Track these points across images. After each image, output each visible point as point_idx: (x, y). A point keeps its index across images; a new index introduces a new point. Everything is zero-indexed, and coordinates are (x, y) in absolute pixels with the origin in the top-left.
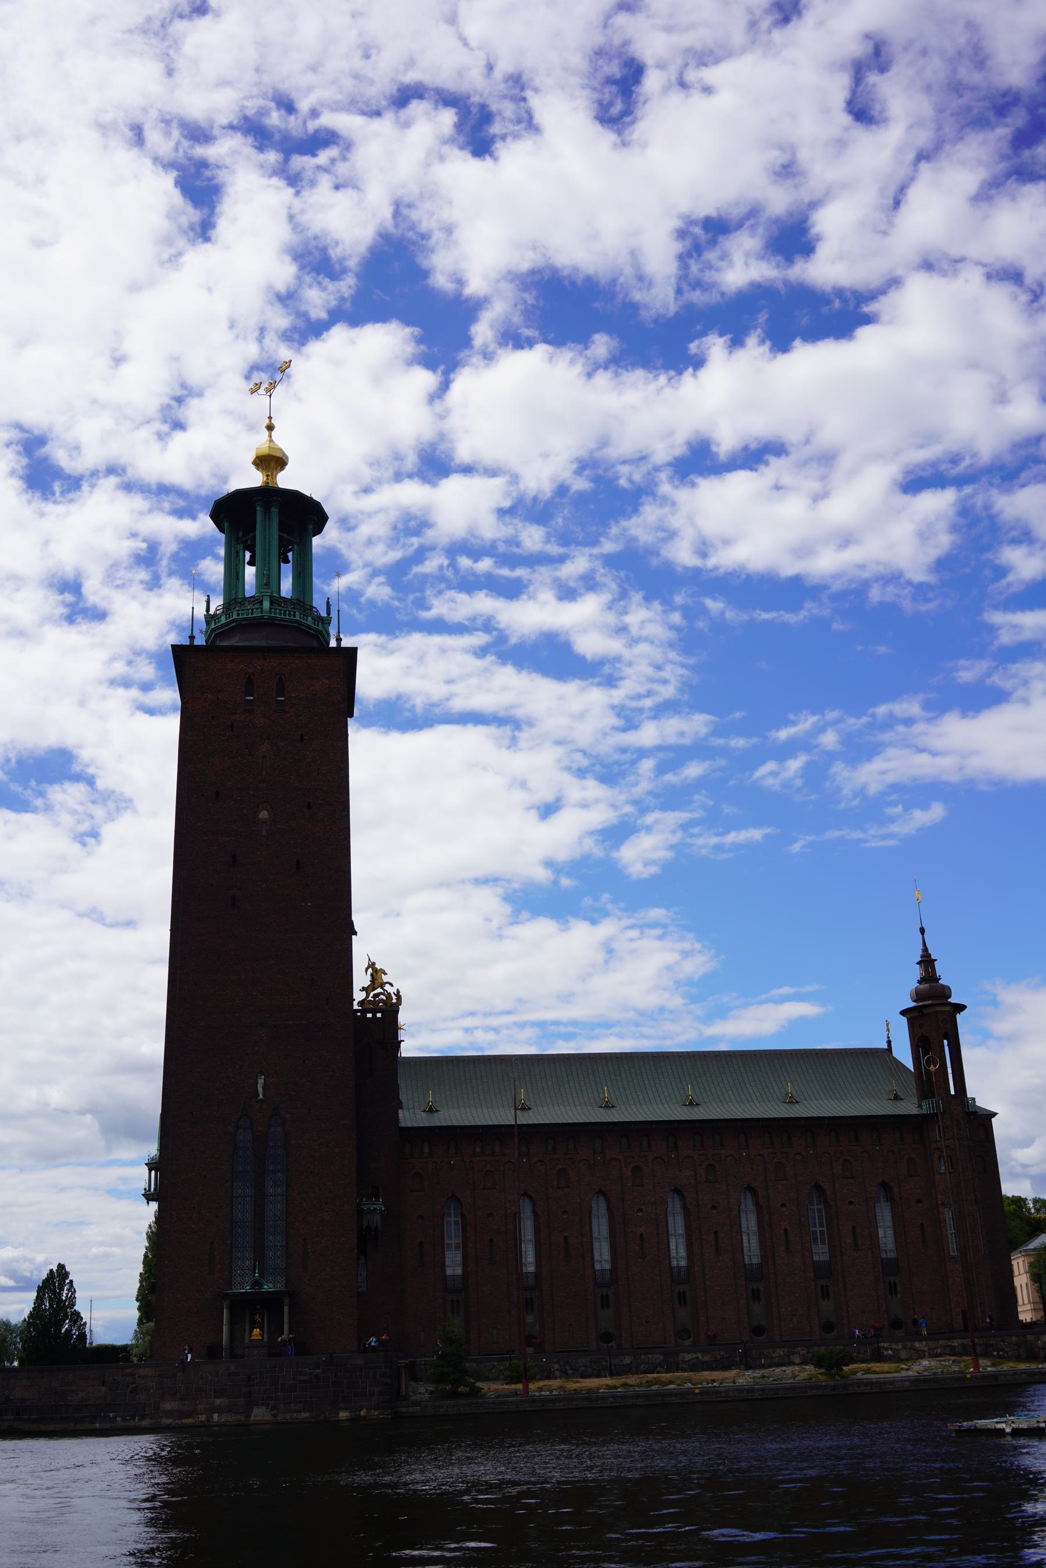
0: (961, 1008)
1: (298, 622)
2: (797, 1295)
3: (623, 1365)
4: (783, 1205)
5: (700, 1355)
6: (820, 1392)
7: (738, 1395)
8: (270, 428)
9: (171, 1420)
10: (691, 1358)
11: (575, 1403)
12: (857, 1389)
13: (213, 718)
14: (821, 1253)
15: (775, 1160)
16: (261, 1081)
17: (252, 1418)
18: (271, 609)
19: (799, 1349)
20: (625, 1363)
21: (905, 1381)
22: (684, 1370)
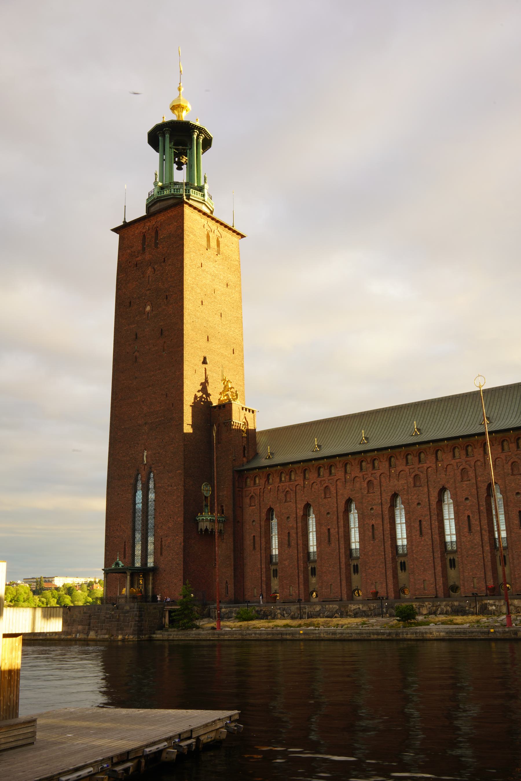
1: (173, 194)
3: (315, 612)
4: (467, 499)
5: (361, 606)
6: (380, 637)
7: (326, 636)
8: (180, 90)
9: (64, 636)
10: (355, 608)
11: (235, 636)
13: (129, 262)
15: (461, 467)
16: (145, 454)
17: (89, 637)
18: (158, 192)
19: (427, 603)
21: (441, 632)
22: (350, 616)
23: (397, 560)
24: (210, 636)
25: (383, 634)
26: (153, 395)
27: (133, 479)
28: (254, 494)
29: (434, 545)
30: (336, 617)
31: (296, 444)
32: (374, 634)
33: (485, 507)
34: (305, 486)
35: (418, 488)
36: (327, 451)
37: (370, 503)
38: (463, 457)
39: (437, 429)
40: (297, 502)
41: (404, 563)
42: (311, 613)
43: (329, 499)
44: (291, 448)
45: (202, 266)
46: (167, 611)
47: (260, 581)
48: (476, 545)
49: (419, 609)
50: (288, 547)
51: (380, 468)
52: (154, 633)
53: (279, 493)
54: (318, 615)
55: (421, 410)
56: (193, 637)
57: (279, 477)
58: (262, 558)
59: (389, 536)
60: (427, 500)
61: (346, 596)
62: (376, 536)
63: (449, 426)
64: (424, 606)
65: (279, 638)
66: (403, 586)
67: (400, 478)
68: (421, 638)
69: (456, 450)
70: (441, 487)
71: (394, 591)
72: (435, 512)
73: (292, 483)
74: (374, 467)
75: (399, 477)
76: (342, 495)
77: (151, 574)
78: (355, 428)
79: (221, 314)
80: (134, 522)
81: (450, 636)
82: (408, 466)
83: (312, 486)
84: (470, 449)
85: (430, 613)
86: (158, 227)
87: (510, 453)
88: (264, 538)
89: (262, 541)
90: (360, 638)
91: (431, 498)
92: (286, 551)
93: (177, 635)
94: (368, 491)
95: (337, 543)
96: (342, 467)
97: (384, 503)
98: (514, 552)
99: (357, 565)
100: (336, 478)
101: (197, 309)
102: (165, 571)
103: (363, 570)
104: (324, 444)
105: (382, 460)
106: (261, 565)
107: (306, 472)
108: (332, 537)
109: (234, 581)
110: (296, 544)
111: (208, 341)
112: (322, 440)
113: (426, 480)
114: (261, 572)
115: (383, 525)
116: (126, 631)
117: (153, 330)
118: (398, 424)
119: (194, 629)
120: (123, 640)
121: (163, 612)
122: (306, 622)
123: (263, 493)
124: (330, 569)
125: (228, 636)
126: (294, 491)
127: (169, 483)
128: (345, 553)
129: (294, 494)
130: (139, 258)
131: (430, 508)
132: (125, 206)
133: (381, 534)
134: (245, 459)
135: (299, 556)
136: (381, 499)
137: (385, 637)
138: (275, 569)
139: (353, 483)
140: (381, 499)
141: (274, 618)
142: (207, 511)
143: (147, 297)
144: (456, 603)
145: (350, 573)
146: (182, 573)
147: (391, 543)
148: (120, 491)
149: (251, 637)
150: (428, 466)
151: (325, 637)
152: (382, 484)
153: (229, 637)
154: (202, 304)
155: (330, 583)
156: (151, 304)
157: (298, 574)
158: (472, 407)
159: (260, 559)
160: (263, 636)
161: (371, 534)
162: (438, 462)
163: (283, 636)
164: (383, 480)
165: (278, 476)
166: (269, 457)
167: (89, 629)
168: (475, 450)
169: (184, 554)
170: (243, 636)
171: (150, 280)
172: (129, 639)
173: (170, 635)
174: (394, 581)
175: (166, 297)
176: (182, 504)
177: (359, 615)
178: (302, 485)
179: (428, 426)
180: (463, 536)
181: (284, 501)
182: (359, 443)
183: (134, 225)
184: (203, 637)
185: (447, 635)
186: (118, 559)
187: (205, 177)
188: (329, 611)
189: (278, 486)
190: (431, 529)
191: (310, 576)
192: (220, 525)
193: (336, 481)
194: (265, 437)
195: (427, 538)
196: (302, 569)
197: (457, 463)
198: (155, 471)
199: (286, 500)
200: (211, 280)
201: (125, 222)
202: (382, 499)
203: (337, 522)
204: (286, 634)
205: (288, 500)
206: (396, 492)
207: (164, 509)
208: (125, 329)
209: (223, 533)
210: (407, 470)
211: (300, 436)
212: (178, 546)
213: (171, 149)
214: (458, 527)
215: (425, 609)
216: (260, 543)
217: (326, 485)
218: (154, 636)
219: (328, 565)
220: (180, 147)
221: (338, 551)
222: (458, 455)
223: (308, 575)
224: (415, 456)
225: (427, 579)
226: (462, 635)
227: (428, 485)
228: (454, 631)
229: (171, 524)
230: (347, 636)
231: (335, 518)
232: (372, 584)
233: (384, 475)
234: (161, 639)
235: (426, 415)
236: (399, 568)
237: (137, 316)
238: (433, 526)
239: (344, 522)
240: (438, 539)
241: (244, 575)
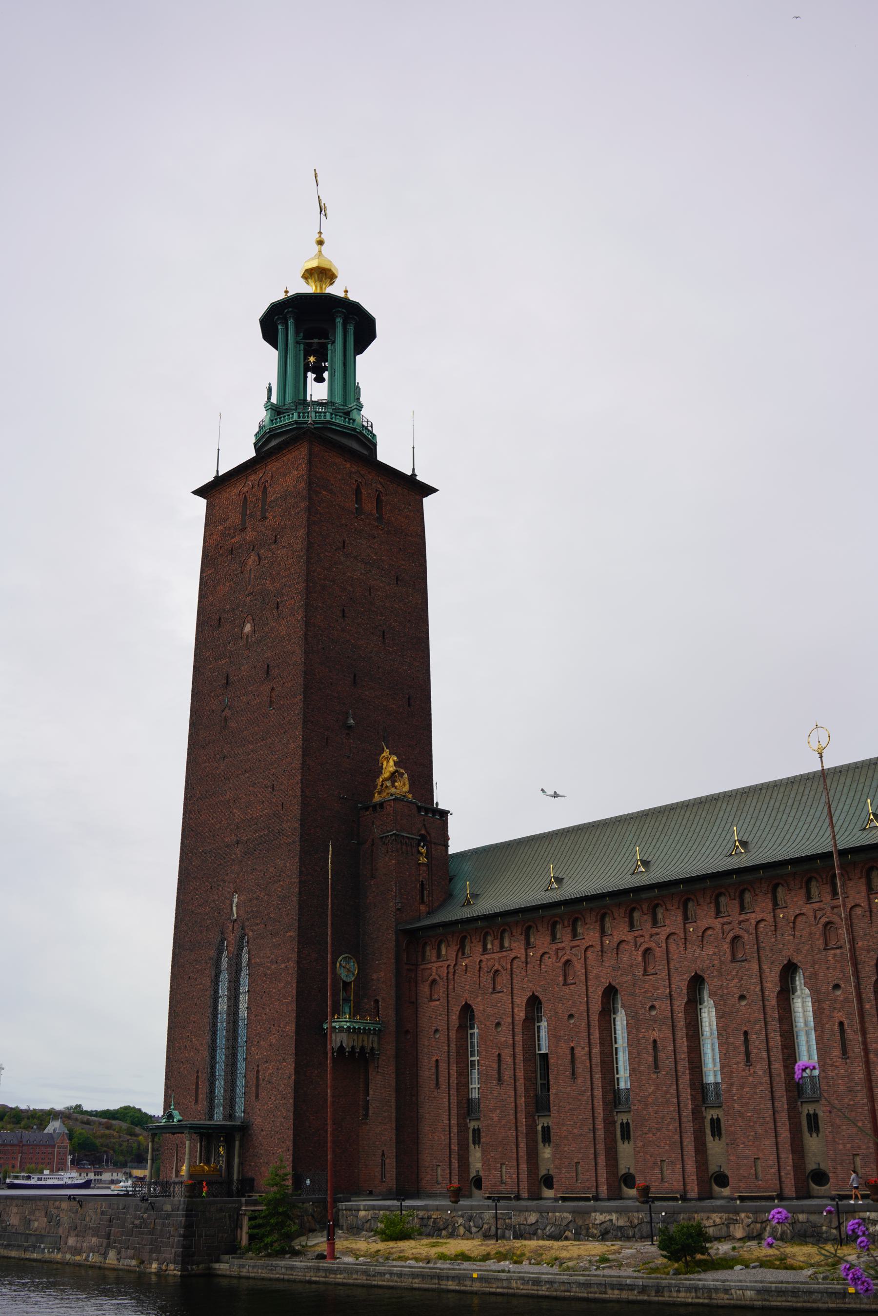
1: (296, 422)
3: (528, 1225)
4: (837, 987)
6: (624, 1295)
7: (522, 1287)
8: (321, 243)
10: (603, 1220)
11: (354, 1276)
12: (675, 1294)
13: (221, 547)
15: (824, 920)
16: (236, 900)
18: (272, 421)
19: (743, 1215)
20: (529, 1222)
21: (748, 1288)
23: (704, 1114)
24: (312, 1274)
25: (631, 1288)
27: (214, 948)
28: (437, 977)
29: (775, 1084)
30: (567, 1239)
31: (521, 876)
32: (613, 1286)
33: (874, 1003)
34: (529, 960)
35: (739, 964)
36: (573, 889)
37: (650, 994)
38: (827, 898)
39: (778, 842)
40: (515, 992)
42: (519, 1227)
43: (571, 987)
44: (510, 884)
45: (344, 547)
46: (245, 1214)
47: (448, 1152)
48: (857, 1085)
49: (728, 1226)
50: (499, 1084)
51: (667, 922)
52: (218, 1261)
53: (481, 975)
54: (529, 1233)
55: (754, 804)
56: (282, 1274)
57: (481, 943)
58: (451, 1106)
59: (687, 1065)
60: (758, 989)
61: (605, 1187)
62: (661, 1065)
63: (802, 834)
64: (736, 1220)
65: (433, 1286)
66: (717, 1169)
67: (705, 942)
68: (706, 1301)
69: (814, 883)
70: (785, 962)
71: (697, 1179)
72: (774, 1014)
73: (505, 954)
74: (655, 922)
75: (702, 941)
76: (597, 977)
77: (238, 1137)
78: (628, 842)
79: (384, 632)
80: (214, 1032)
81: (765, 1300)
82: (719, 919)
83: (541, 961)
85: (749, 1238)
86: (267, 481)
88: (455, 1065)
89: (451, 1071)
90: (585, 1295)
91: (765, 985)
92: (495, 1093)
93: (254, 1267)
94: (645, 970)
95: (588, 1076)
96: (596, 922)
97: (675, 995)
99: (628, 1124)
100: (584, 944)
101: (332, 625)
102: (262, 1130)
103: (638, 1134)
104: (570, 875)
105: (669, 907)
106: (449, 1120)
107: (531, 932)
108: (578, 1065)
109: (396, 1152)
110: (513, 1077)
111: (355, 682)
112: (566, 868)
113: (755, 946)
114: (450, 1134)
115: (674, 1041)
116: (164, 1255)
117: (255, 667)
118: (707, 832)
119: (288, 1256)
120: (158, 1274)
121: (238, 1217)
122: (500, 1249)
123: (454, 975)
124: (575, 1131)
125: (342, 1276)
126: (509, 970)
127: (272, 956)
128: (604, 1097)
129: (509, 977)
131: (764, 1006)
132: (219, 450)
133: (670, 1060)
134: (423, 908)
135: (518, 1102)
136: (670, 988)
137: (633, 1296)
138: (476, 1127)
139: (617, 954)
140: (670, 988)
141: (451, 1235)
142: (347, 1010)
143: (246, 607)
144: (802, 1217)
145: (615, 1141)
146: (292, 1136)
147: (691, 1080)
148: (192, 972)
149: (384, 1281)
150: (759, 919)
151: (519, 1289)
152: (670, 955)
153: (344, 1278)
154: (344, 616)
155: (576, 1161)
156: (253, 619)
157: (517, 1139)
158: (851, 794)
159: (447, 1108)
160: (405, 1280)
161: (651, 1059)
162: (778, 910)
163: (441, 1282)
164: (673, 947)
165: (480, 941)
166: (469, 902)
168: (850, 884)
169: (295, 1098)
170: (368, 1278)
171: (252, 576)
172: (167, 1272)
173: (243, 1266)
174: (699, 1159)
175: (276, 606)
176: (294, 998)
177: (610, 1235)
178: (523, 959)
179: (764, 836)
180: (832, 1065)
182: (631, 872)
183: (230, 480)
184: (300, 1274)
185: (760, 1297)
186: (172, 1107)
188: (553, 1224)
189: (481, 961)
190: (768, 1050)
191: (541, 1145)
192: (371, 1039)
193: (586, 950)
194: (469, 863)
195: (760, 1068)
196: (523, 1129)
197: (815, 911)
198: (251, 934)
199: (494, 988)
200: (363, 572)
202: (672, 986)
203: (587, 1034)
204: (447, 1278)
205: (499, 988)
206: (698, 972)
207: (263, 1008)
208: (210, 668)
209: (378, 1054)
210: (718, 926)
211: (530, 859)
212: (286, 1081)
213: (300, 344)
214: (821, 1046)
215: (739, 1227)
216: (447, 1075)
217: (566, 958)
218: (216, 1266)
219: (572, 1123)
220: (316, 341)
221: (589, 1094)
222: (817, 894)
223: (537, 1142)
224: (732, 897)
225: (761, 1155)
226: (790, 1299)
227: (759, 957)
228: (773, 1289)
229: (275, 1037)
230: (562, 1288)
231: (584, 1025)
232: (655, 1163)
233: (675, 937)
234: (228, 1273)
235: (762, 814)
236: (708, 1131)
237: (229, 643)
238: (772, 1044)
239: (601, 1033)
240: (782, 1072)
241: (418, 1138)
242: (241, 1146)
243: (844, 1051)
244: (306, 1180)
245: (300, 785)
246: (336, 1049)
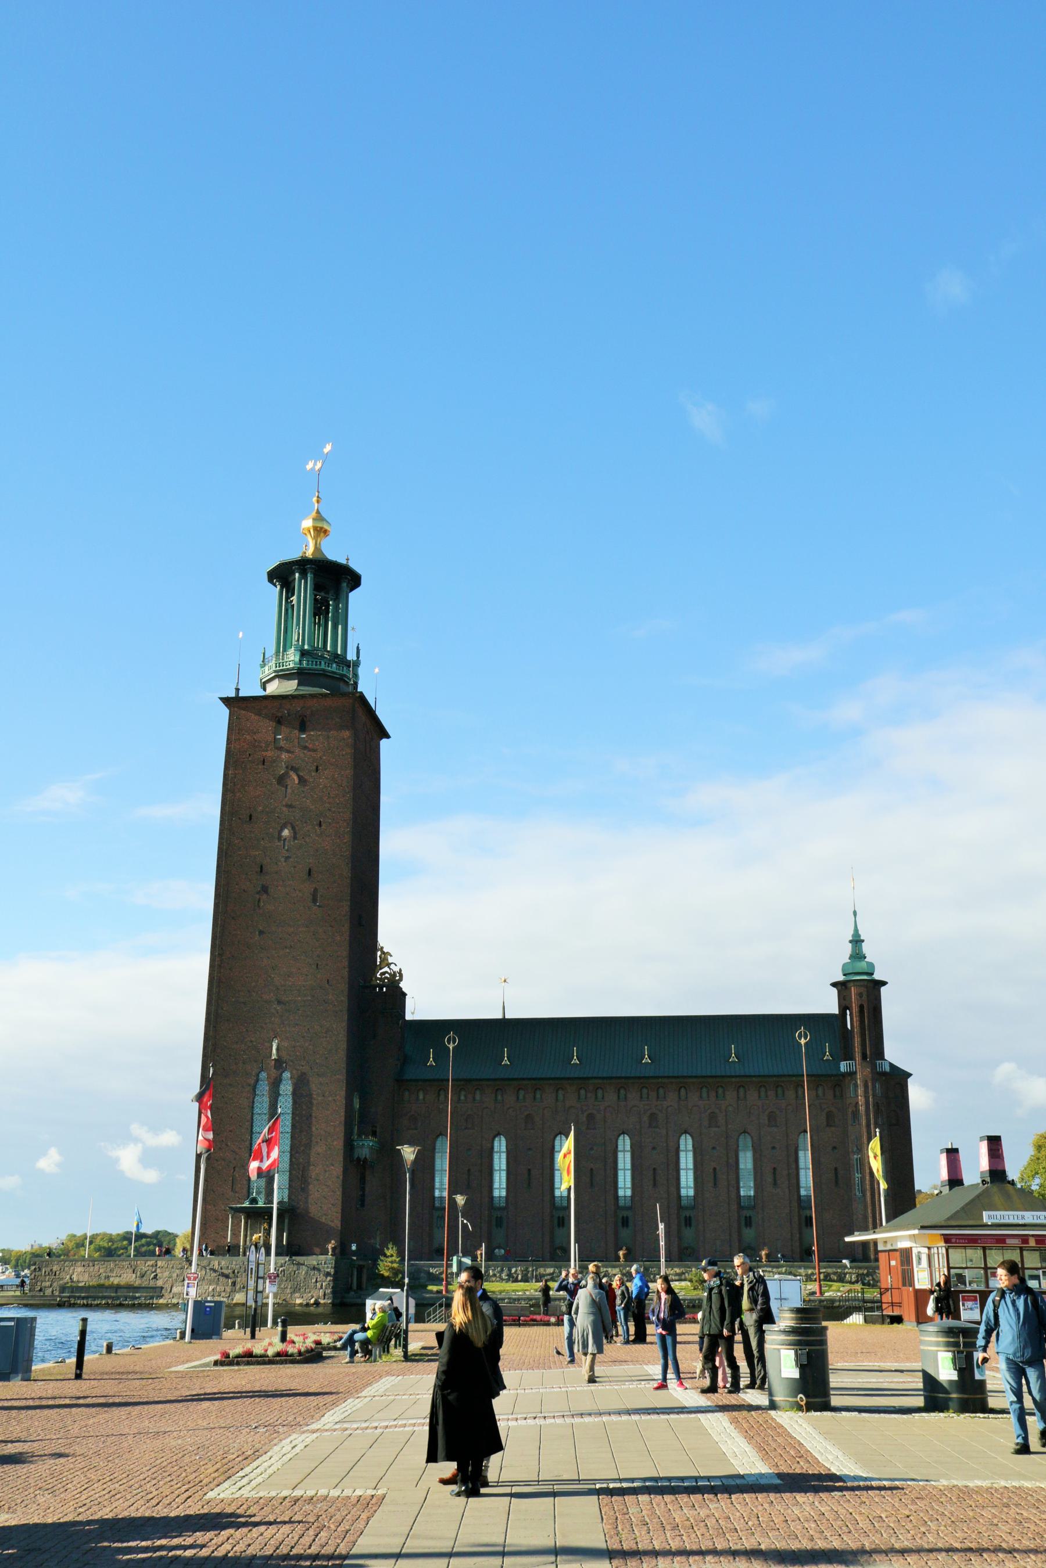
0: (884, 983)
1: (324, 670)
2: (721, 1223)
4: (714, 1148)
13: (250, 755)
14: (747, 1189)
26: (291, 962)
41: (627, 1217)
84: (720, 1090)
87: (767, 1102)
98: (765, 1214)
130: (269, 754)
131: (667, 1155)
167: (234, 1291)
181: (463, 1127)
187: (358, 648)
201: (237, 690)
210: (642, 1106)
217: (528, 1112)
236: (620, 1224)
242: (289, 1223)
243: (715, 1184)
244: (351, 1246)
245: (347, 969)
246: (362, 1159)
